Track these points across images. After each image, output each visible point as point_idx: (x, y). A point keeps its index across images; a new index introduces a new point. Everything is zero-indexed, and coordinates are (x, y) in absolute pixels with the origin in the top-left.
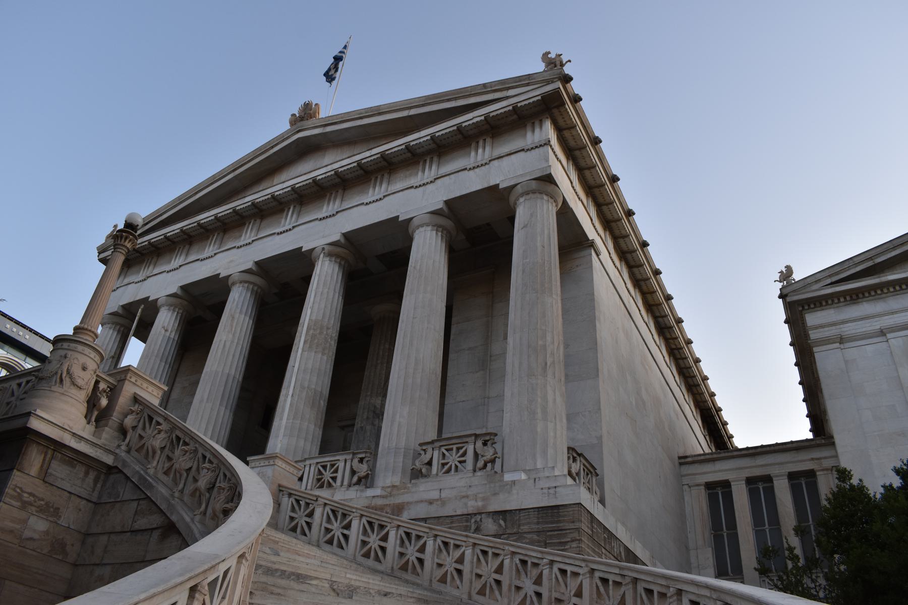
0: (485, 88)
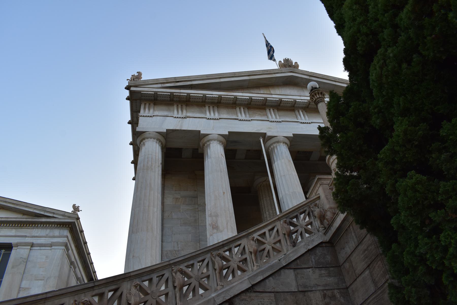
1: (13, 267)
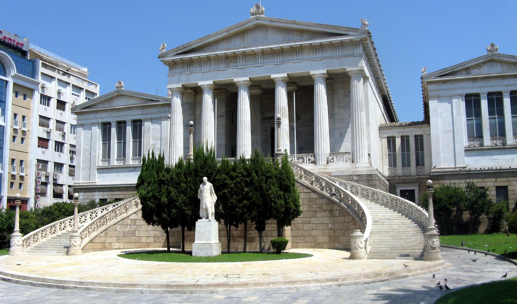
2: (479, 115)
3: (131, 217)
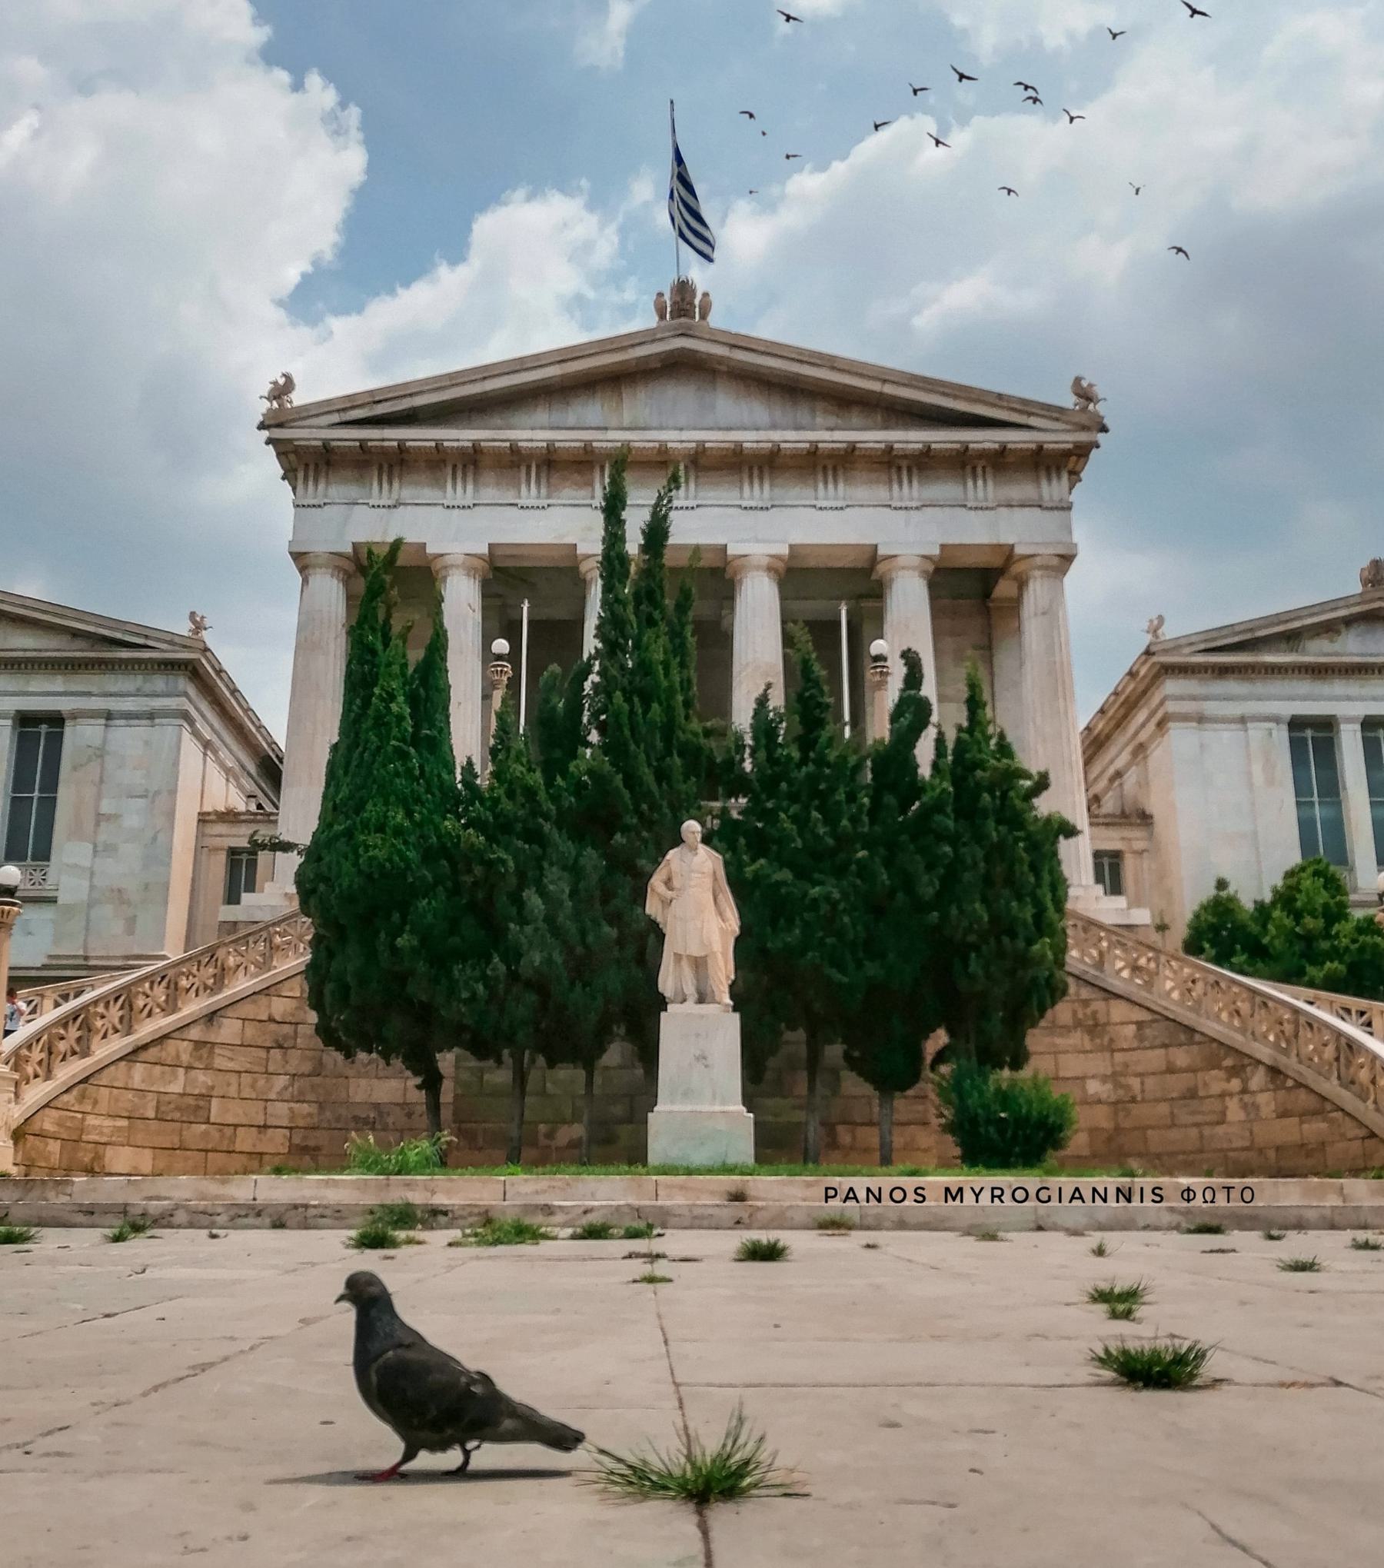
0: (999, 399)
1: (75, 769)
2: (1331, 789)
3: (195, 1033)
